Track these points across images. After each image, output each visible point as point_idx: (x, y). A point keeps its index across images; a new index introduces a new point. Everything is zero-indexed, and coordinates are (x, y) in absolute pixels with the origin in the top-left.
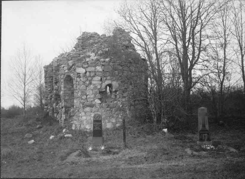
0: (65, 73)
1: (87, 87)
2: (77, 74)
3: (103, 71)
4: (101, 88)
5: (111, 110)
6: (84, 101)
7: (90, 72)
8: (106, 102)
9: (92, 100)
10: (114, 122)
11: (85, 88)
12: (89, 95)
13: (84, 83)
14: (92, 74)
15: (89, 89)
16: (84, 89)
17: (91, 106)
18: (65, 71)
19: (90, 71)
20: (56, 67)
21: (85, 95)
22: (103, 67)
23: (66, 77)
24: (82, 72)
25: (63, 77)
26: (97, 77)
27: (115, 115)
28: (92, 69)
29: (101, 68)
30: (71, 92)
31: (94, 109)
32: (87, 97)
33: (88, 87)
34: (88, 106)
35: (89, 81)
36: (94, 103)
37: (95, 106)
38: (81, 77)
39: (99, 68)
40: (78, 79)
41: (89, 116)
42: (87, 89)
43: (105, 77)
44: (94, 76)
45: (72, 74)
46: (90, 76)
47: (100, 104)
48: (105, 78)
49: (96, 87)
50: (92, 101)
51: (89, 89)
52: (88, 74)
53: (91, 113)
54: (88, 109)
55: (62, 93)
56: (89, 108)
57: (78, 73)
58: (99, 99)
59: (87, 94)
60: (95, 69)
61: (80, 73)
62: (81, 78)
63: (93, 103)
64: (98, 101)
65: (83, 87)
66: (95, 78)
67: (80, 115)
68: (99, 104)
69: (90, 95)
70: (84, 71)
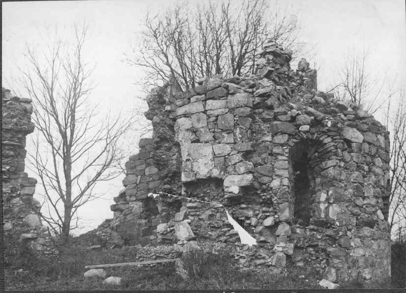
45: (329, 139)
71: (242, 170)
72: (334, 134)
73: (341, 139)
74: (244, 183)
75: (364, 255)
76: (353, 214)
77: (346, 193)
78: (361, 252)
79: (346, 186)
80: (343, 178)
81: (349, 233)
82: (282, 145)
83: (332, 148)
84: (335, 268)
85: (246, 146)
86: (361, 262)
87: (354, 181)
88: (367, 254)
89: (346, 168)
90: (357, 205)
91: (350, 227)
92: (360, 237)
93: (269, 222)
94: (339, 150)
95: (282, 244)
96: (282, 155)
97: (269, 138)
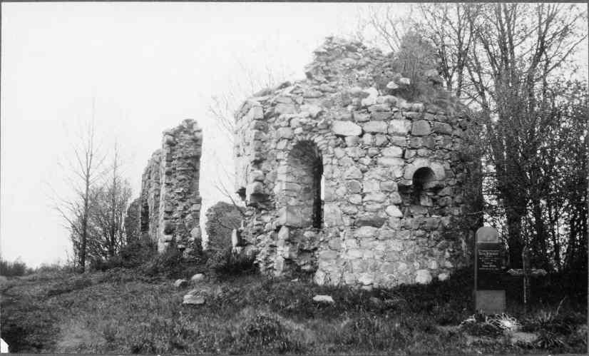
0: (295, 135)
1: (363, 172)
2: (335, 137)
3: (410, 132)
4: (402, 177)
5: (428, 235)
6: (356, 210)
7: (374, 134)
8: (412, 217)
9: (379, 206)
10: (433, 268)
11: (357, 174)
12: (370, 193)
13: (356, 161)
14: (380, 140)
15: (371, 179)
16: (356, 179)
17: (376, 223)
18: (294, 129)
19: (375, 131)
20: (259, 120)
21: (359, 193)
22: (409, 123)
23: (294, 146)
24: (351, 134)
25: (287, 145)
26: (393, 147)
27: (435, 251)
28: (378, 127)
29: (405, 125)
30: (303, 188)
31: (383, 231)
32: (363, 198)
33: (365, 174)
34: (366, 223)
35: (372, 157)
36: (383, 215)
37: (386, 224)
38: (346, 146)
39: (400, 126)
40: (339, 151)
41: (371, 250)
42: (366, 179)
43: (413, 148)
44: (383, 146)
45: (321, 137)
46: (374, 145)
47: (401, 218)
48: (413, 152)
49: (391, 173)
50: (377, 211)
51: (371, 179)
52: (367, 139)
53: (377, 242)
54: (366, 231)
55: (281, 187)
56: (370, 228)
57: (338, 136)
58: (396, 205)
60: (388, 127)
61: (345, 134)
62: (347, 149)
63: (382, 217)
64: (395, 212)
65: (353, 171)
66: (386, 149)
67: (343, 245)
68: (397, 217)
69: (373, 193)
70: (357, 130)
73: (332, 135)
75: (361, 258)
77: (338, 191)
78: (357, 254)
79: (338, 184)
82: (283, 151)
83: (323, 146)
84: (324, 271)
86: (356, 265)
87: (349, 178)
88: (365, 257)
89: (339, 165)
90: (353, 204)
91: (342, 228)
94: (330, 148)
96: (283, 160)
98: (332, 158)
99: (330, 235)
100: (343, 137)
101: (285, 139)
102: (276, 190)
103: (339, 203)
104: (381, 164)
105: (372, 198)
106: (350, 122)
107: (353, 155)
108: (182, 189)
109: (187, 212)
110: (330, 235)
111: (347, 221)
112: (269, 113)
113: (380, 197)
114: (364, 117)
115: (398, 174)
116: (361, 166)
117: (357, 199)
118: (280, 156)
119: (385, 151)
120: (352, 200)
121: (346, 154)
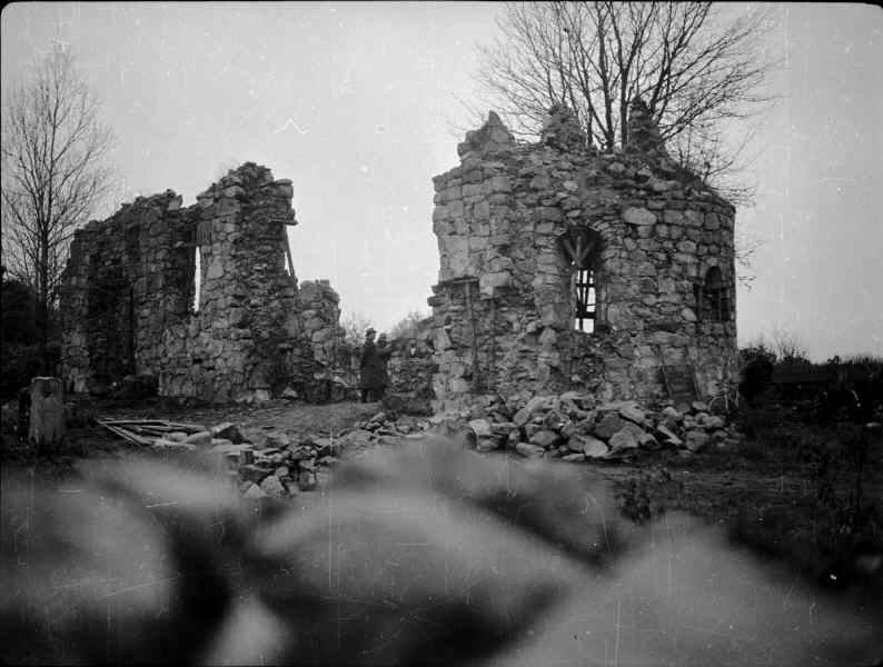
3: (703, 225)
9: (674, 309)
12: (666, 294)
13: (649, 256)
14: (676, 232)
34: (662, 327)
38: (639, 237)
45: (606, 225)
46: (669, 238)
53: (672, 350)
54: (662, 337)
57: (628, 224)
58: (691, 308)
59: (660, 291)
65: (646, 267)
67: (637, 353)
70: (652, 218)
71: (497, 268)
72: (611, 217)
74: (499, 284)
76: (641, 317)
80: (624, 271)
81: (632, 339)
82: (547, 235)
85: (503, 239)
89: (629, 259)
90: (646, 305)
92: (650, 344)
93: (531, 327)
94: (619, 238)
95: (546, 354)
96: (546, 247)
97: (530, 228)
98: (621, 250)
99: (620, 340)
100: (634, 226)
101: (551, 221)
102: (538, 282)
103: (631, 304)
104: (676, 260)
105: (668, 299)
106: (643, 210)
107: (646, 248)
108: (265, 265)
109: (272, 298)
110: (620, 340)
111: (641, 324)
112: (520, 186)
113: (675, 298)
114: (660, 205)
115: (693, 273)
116: (655, 262)
117: (651, 300)
118: (541, 241)
119: (681, 246)
120: (646, 301)
121: (638, 247)
